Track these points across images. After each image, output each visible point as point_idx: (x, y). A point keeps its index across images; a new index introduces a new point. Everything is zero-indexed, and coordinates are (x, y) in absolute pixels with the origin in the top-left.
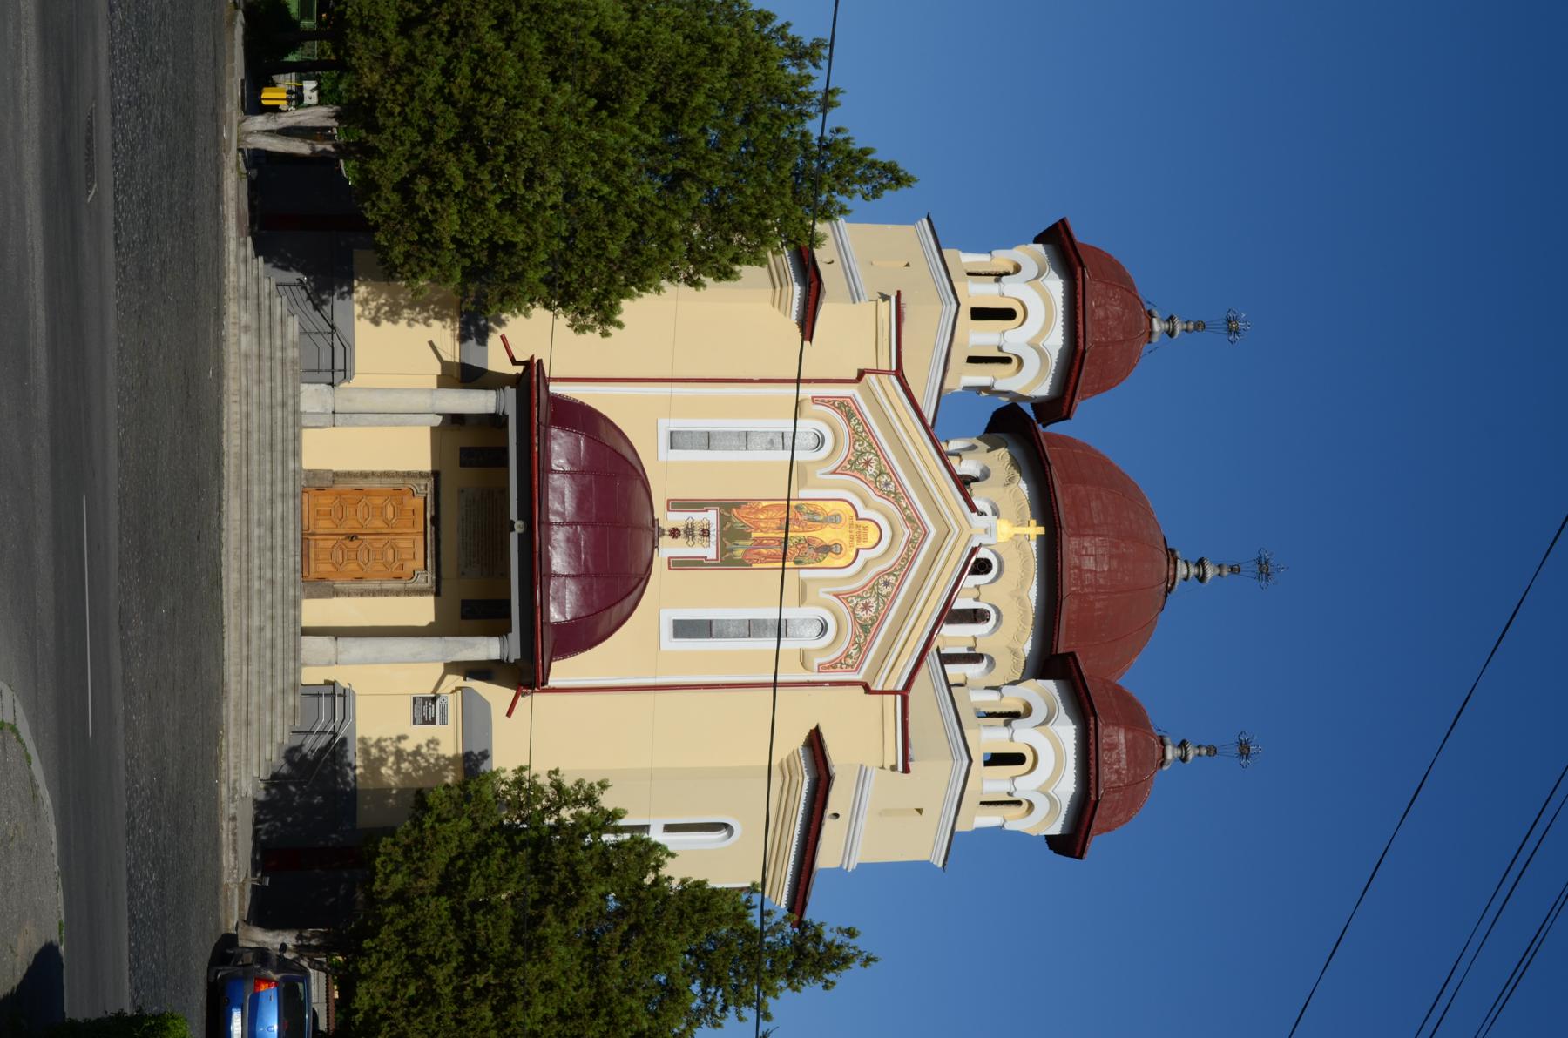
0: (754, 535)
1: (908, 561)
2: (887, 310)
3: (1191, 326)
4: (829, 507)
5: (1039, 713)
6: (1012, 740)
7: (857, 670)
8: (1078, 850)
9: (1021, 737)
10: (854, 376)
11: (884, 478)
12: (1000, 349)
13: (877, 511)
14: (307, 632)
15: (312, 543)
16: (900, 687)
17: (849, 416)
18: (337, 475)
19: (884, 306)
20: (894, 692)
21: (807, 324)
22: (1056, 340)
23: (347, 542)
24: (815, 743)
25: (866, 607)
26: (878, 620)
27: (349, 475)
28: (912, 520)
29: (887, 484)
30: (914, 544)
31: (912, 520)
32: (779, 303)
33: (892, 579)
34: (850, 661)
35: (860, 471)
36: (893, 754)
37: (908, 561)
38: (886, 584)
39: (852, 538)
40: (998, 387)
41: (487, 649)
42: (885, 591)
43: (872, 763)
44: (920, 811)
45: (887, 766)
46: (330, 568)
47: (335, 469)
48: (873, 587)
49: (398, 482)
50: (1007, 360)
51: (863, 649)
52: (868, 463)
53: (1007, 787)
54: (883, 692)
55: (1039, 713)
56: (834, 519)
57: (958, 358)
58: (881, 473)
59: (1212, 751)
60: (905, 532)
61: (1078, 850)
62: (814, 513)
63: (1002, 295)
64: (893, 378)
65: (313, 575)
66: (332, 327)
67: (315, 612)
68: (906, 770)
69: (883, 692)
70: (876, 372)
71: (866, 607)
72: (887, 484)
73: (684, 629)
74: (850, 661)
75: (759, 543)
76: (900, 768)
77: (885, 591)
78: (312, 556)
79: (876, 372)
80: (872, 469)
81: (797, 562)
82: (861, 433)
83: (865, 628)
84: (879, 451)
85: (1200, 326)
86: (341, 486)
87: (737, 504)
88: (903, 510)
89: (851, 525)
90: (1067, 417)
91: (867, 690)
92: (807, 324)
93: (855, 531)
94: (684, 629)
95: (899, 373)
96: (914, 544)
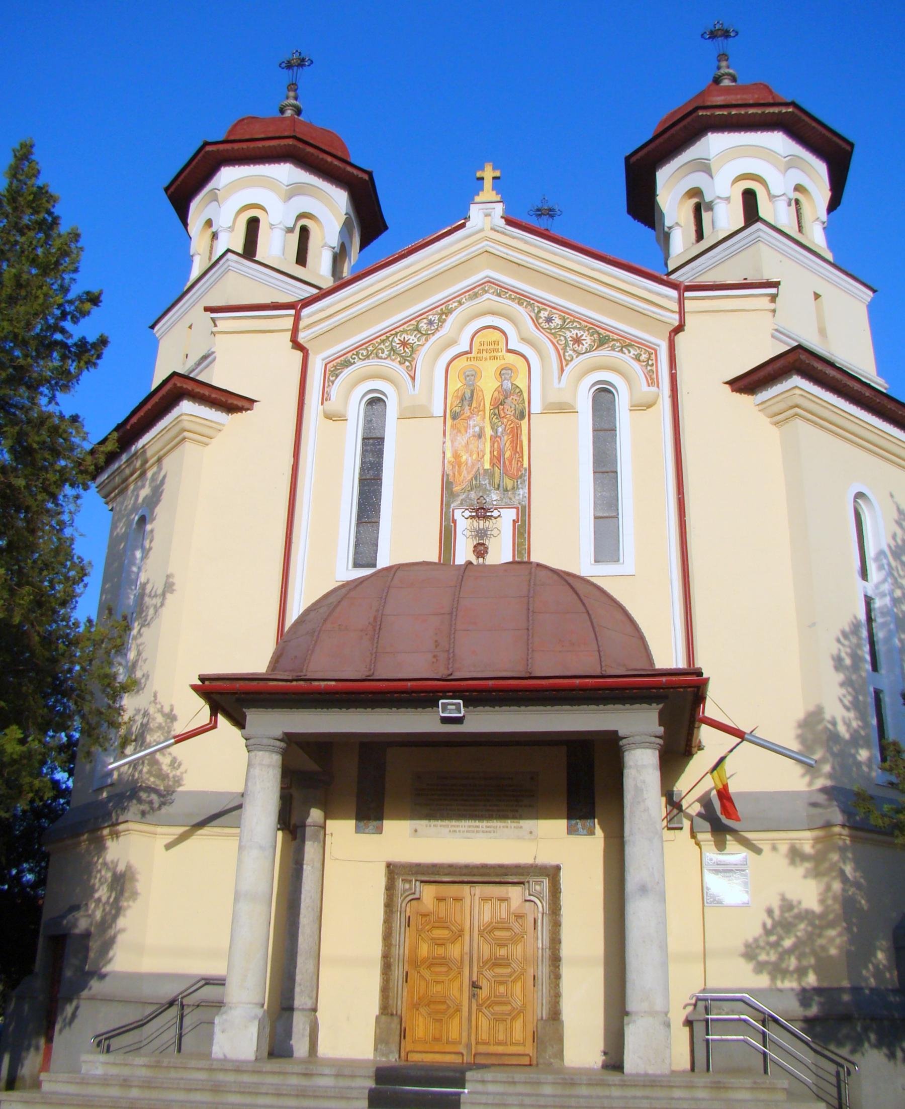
0: (487, 466)
1: (522, 298)
2: (226, 322)
3: (292, 94)
4: (456, 385)
5: (697, 180)
6: (728, 199)
7: (653, 352)
8: (844, 145)
9: (724, 190)
10: (299, 355)
11: (423, 325)
12: (290, 230)
13: (459, 331)
14: (614, 1062)
15: (482, 1049)
16: (674, 293)
17: (347, 364)
18: (385, 1008)
19: (222, 325)
20: (681, 301)
21: (230, 403)
22: (285, 173)
23: (484, 993)
24: (750, 383)
25: (578, 341)
26: (593, 327)
27: (385, 990)
28: (473, 292)
29: (431, 323)
30: (502, 290)
31: (473, 292)
32: (204, 439)
33: (544, 314)
34: (644, 357)
35: (413, 351)
36: (758, 300)
37: (522, 298)
38: (549, 320)
39: (495, 358)
40: (334, 240)
41: (642, 767)
42: (557, 321)
43: (767, 323)
44: (817, 296)
45: (772, 306)
46: (518, 1024)
47: (376, 1010)
48: (553, 334)
49: (398, 921)
50: (304, 231)
51: (626, 343)
52: (404, 344)
53: (782, 204)
54: (682, 312)
55: (697, 180)
56: (471, 377)
57: (298, 271)
58: (417, 329)
59: (723, 56)
60: (488, 299)
61: (844, 145)
62: (463, 399)
63: (231, 229)
64: (305, 312)
65: (529, 1049)
66: (171, 1004)
67: (582, 1047)
68: (776, 285)
69: (682, 312)
70: (295, 330)
71: (578, 341)
72: (431, 323)
73: (607, 546)
74: (644, 357)
75: (497, 459)
76: (773, 291)
77: (557, 321)
78: (500, 1049)
79: (295, 330)
80: (412, 339)
81: (522, 416)
82: (368, 349)
83: (602, 342)
84: (392, 332)
85: (293, 86)
86: (401, 1003)
87: (447, 486)
88: (460, 303)
89: (476, 359)
90: (370, 174)
91: (679, 328)
92: (230, 403)
93: (484, 355)
94: (607, 546)
95: (298, 306)
96: (502, 290)
